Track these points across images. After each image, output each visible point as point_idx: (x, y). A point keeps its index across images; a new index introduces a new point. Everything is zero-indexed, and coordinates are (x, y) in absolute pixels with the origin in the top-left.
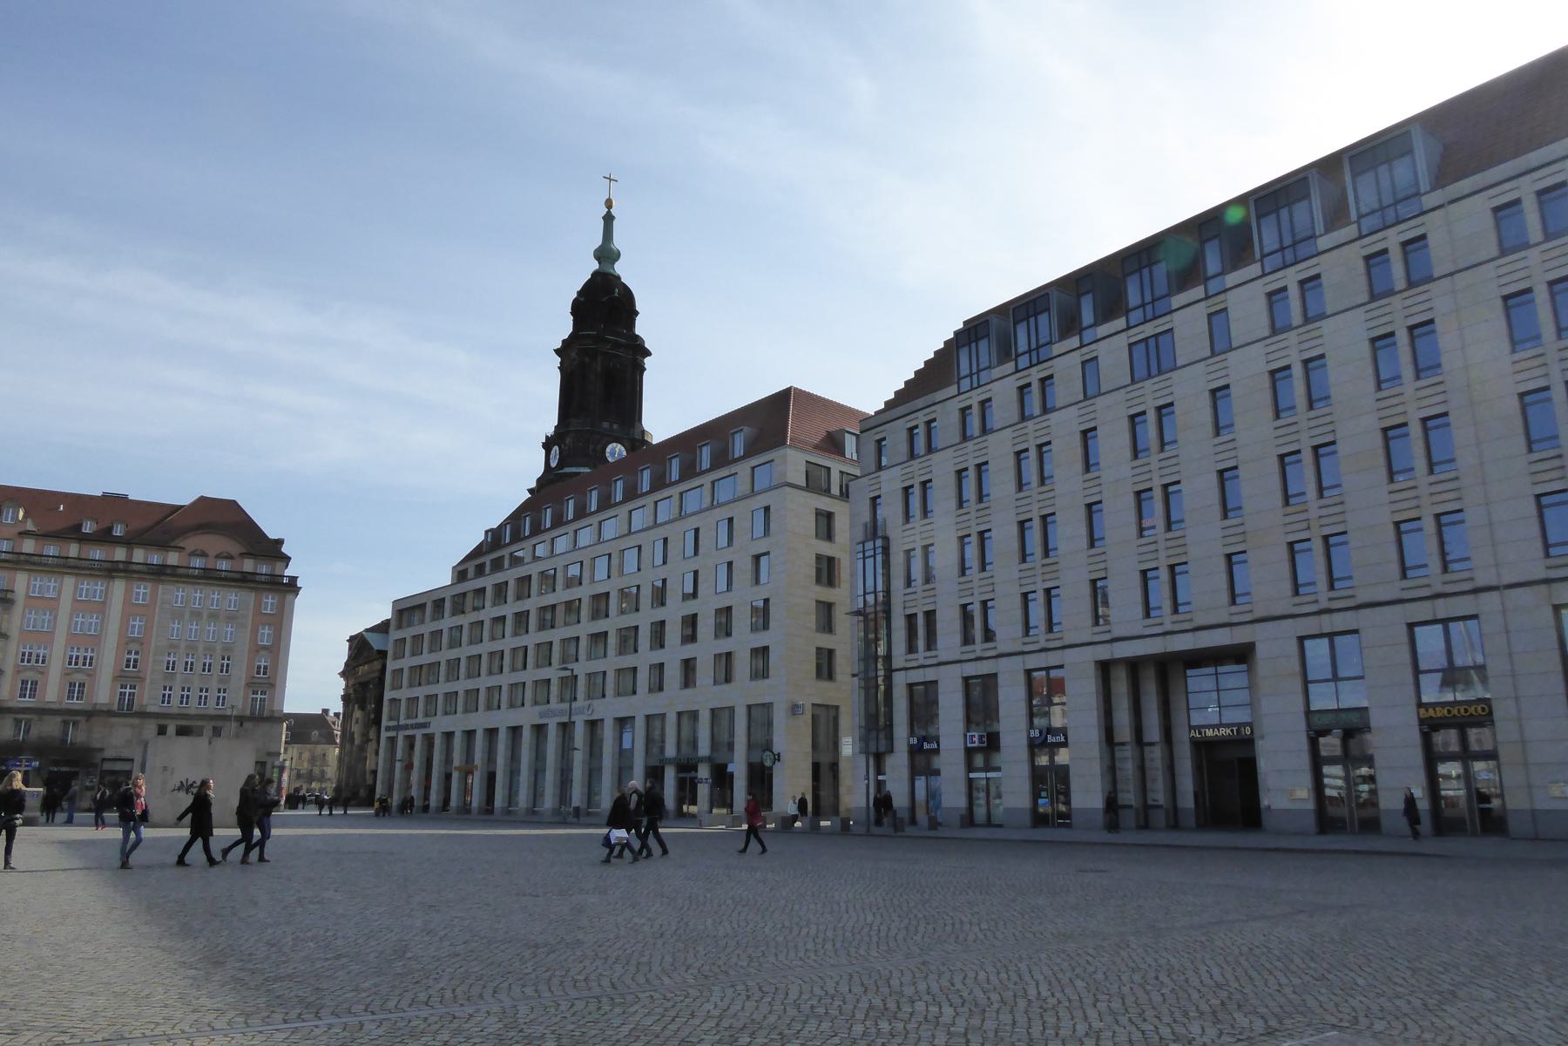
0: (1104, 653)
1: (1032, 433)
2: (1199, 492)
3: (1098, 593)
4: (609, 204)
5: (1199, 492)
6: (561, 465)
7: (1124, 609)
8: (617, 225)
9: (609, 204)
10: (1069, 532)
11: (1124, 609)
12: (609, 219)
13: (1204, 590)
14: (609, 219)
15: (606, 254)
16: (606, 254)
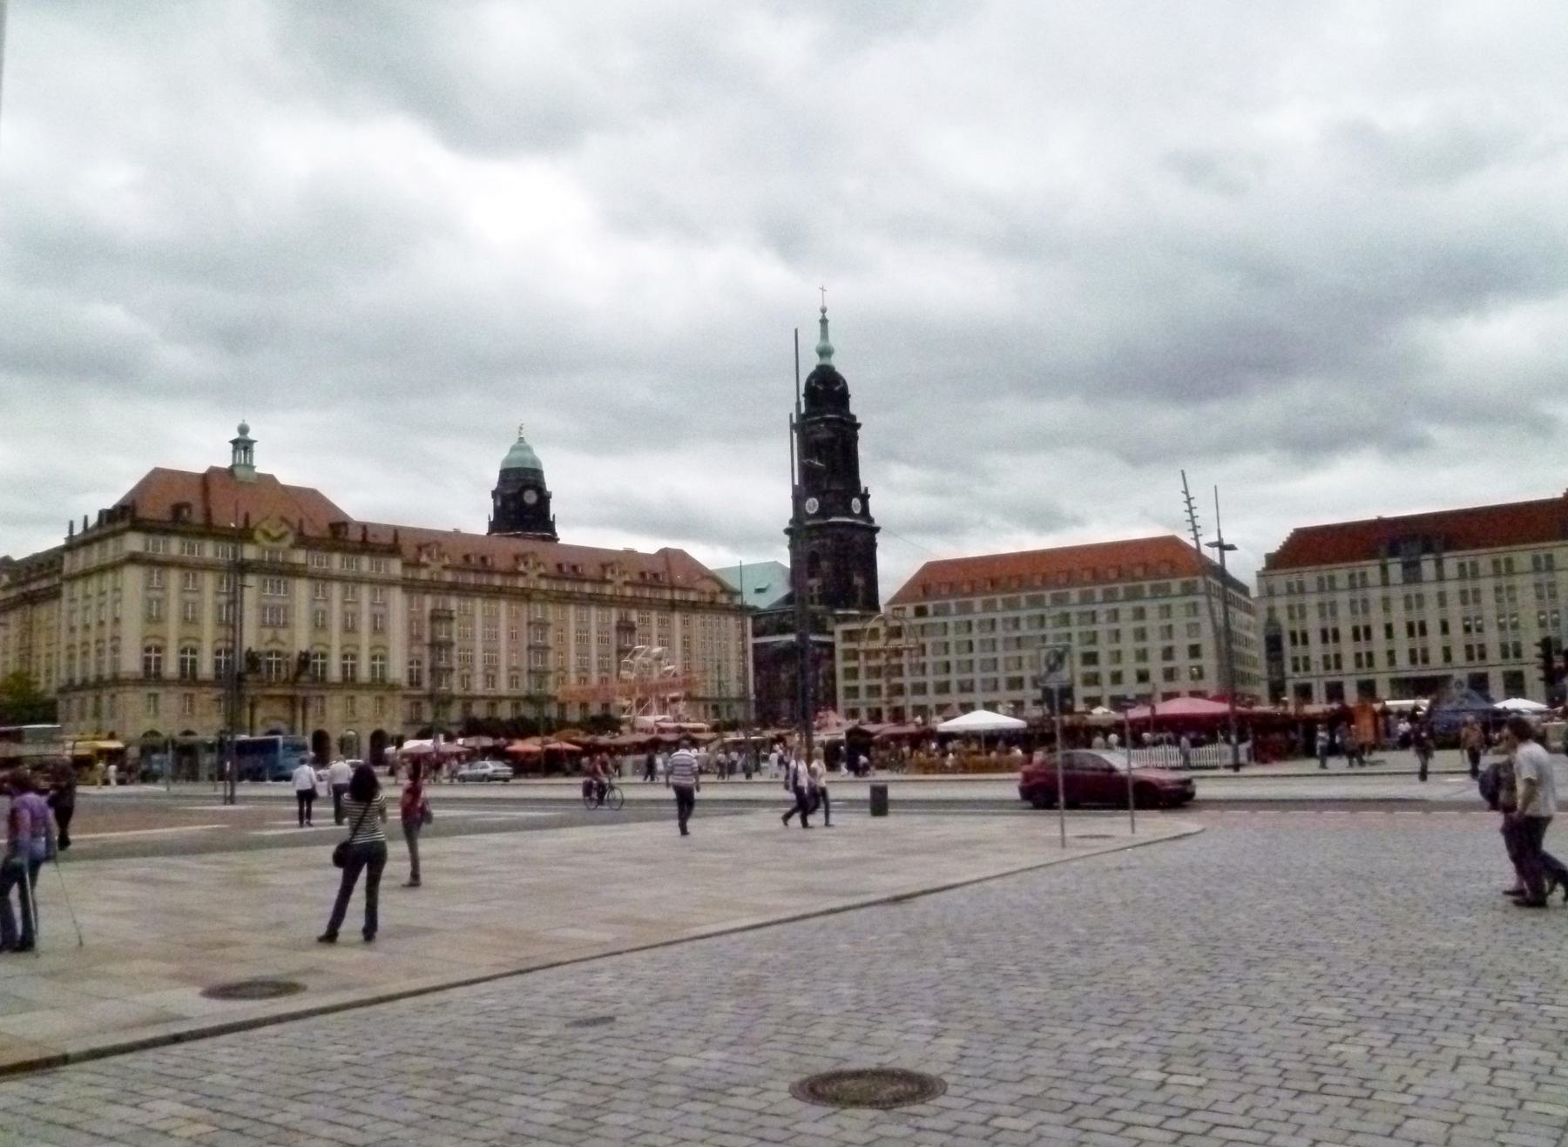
0: (1393, 676)
1: (1359, 595)
2: (1433, 626)
3: (1391, 654)
4: (824, 311)
5: (1433, 626)
6: (823, 512)
7: (1403, 660)
8: (830, 325)
9: (824, 311)
10: (1378, 633)
11: (1403, 660)
12: (824, 322)
13: (1436, 656)
14: (824, 322)
15: (825, 352)
16: (825, 352)
